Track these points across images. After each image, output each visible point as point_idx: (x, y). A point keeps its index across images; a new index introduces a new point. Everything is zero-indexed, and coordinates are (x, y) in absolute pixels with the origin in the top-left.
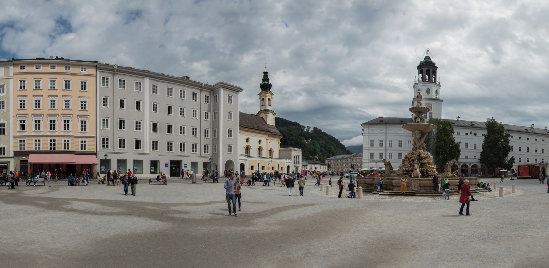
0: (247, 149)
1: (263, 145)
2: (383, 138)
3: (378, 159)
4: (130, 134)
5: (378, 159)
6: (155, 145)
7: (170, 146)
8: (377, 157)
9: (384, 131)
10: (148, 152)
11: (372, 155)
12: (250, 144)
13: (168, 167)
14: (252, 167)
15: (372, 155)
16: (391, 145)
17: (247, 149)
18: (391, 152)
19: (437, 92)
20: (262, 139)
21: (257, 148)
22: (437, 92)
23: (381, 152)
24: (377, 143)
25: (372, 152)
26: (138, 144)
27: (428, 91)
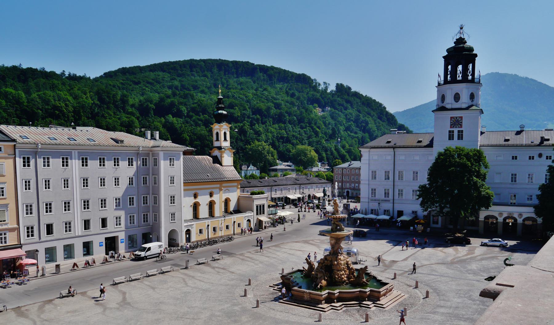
0: (196, 207)
1: (216, 198)
2: (390, 168)
3: (383, 197)
4: (57, 218)
5: (383, 197)
6: (87, 224)
7: (104, 222)
8: (380, 194)
9: (390, 158)
10: (80, 234)
11: (374, 191)
12: (199, 199)
13: (102, 245)
14: (201, 231)
15: (374, 191)
16: (401, 177)
17: (196, 207)
18: (400, 188)
19: (472, 97)
20: (213, 190)
21: (208, 202)
22: (472, 97)
23: (387, 187)
24: (381, 175)
25: (374, 187)
26: (68, 226)
27: (457, 97)
